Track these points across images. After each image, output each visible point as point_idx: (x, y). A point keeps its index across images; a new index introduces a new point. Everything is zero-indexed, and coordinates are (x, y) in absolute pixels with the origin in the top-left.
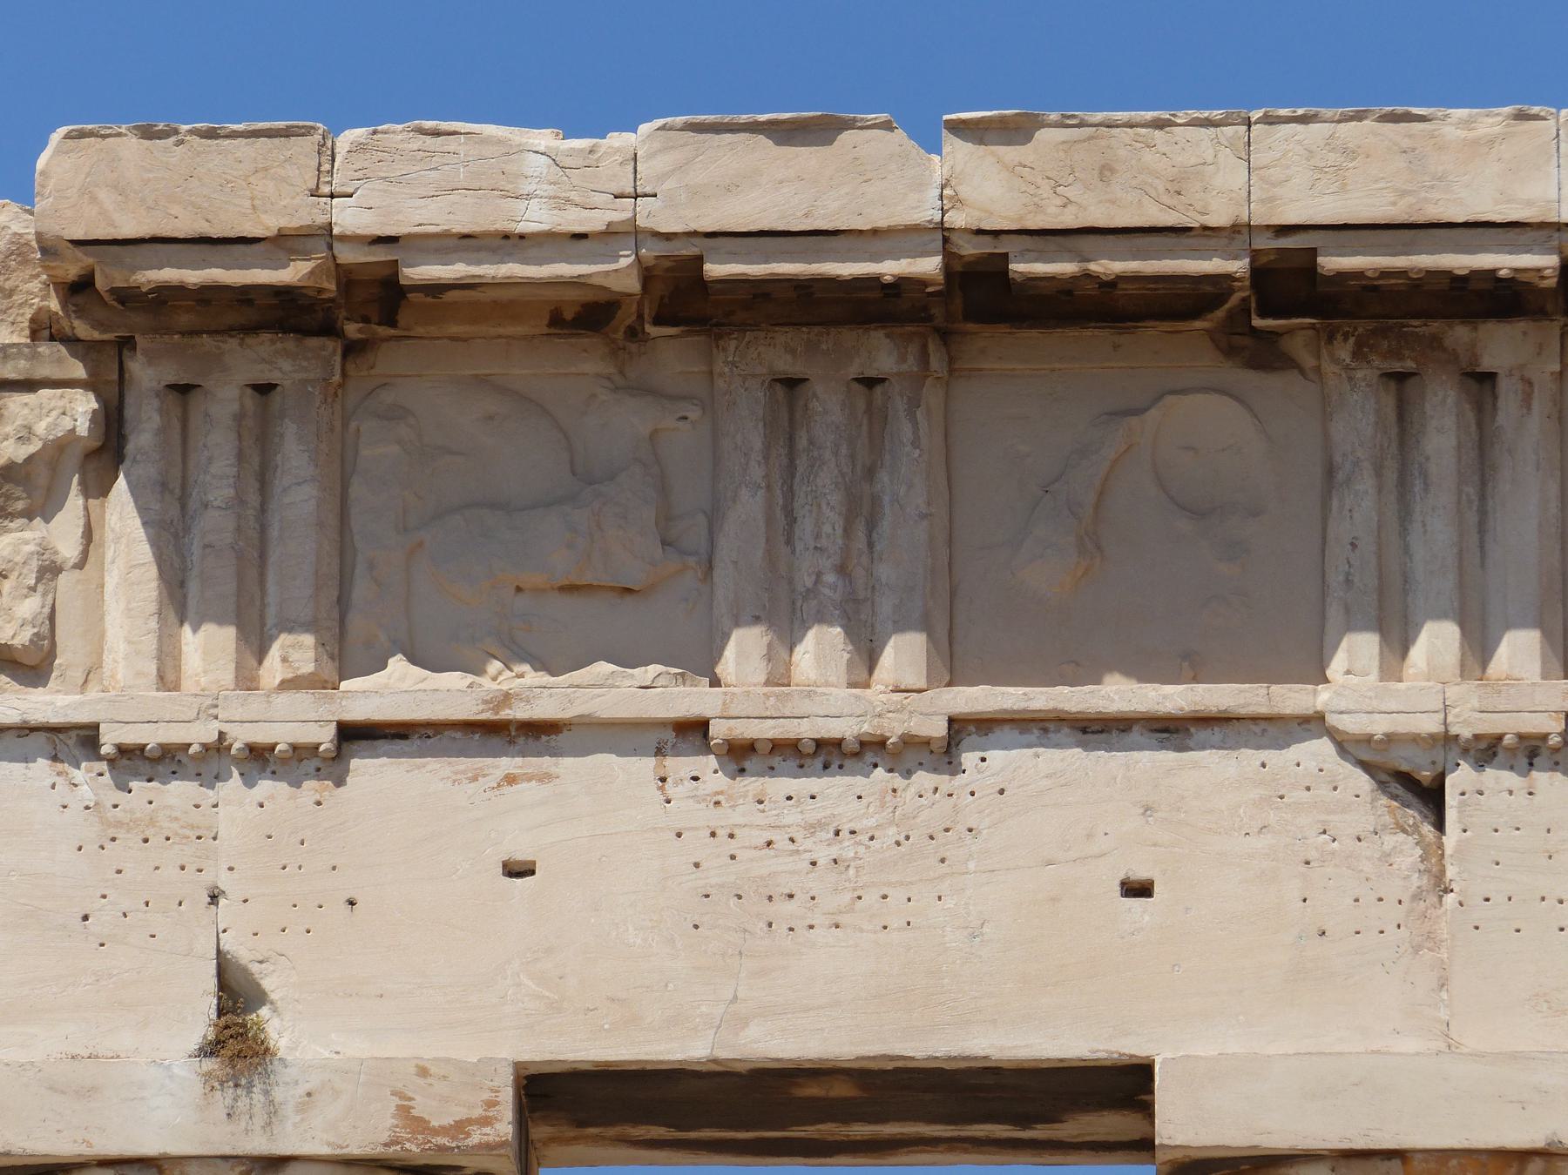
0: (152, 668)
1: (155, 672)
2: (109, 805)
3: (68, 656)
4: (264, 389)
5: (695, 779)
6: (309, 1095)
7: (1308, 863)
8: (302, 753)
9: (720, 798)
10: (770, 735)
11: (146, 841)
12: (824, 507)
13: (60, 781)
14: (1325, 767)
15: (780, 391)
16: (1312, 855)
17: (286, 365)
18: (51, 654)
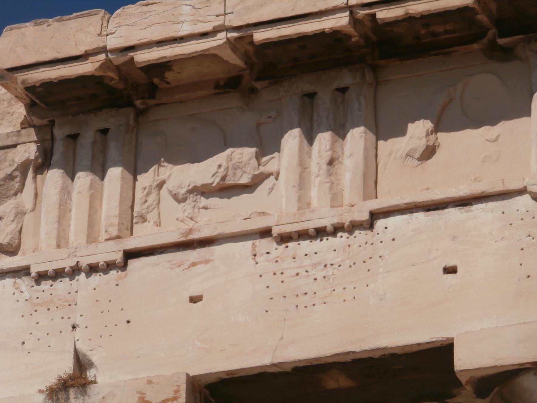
0: (54, 242)
1: (55, 244)
2: (35, 298)
3: (27, 243)
4: (104, 132)
5: (268, 253)
6: (103, 398)
7: (522, 249)
8: (110, 266)
9: (278, 259)
10: (296, 229)
11: (49, 309)
12: (322, 139)
13: (16, 291)
14: (529, 209)
15: (307, 99)
16: (524, 246)
17: (112, 120)
18: (19, 246)
